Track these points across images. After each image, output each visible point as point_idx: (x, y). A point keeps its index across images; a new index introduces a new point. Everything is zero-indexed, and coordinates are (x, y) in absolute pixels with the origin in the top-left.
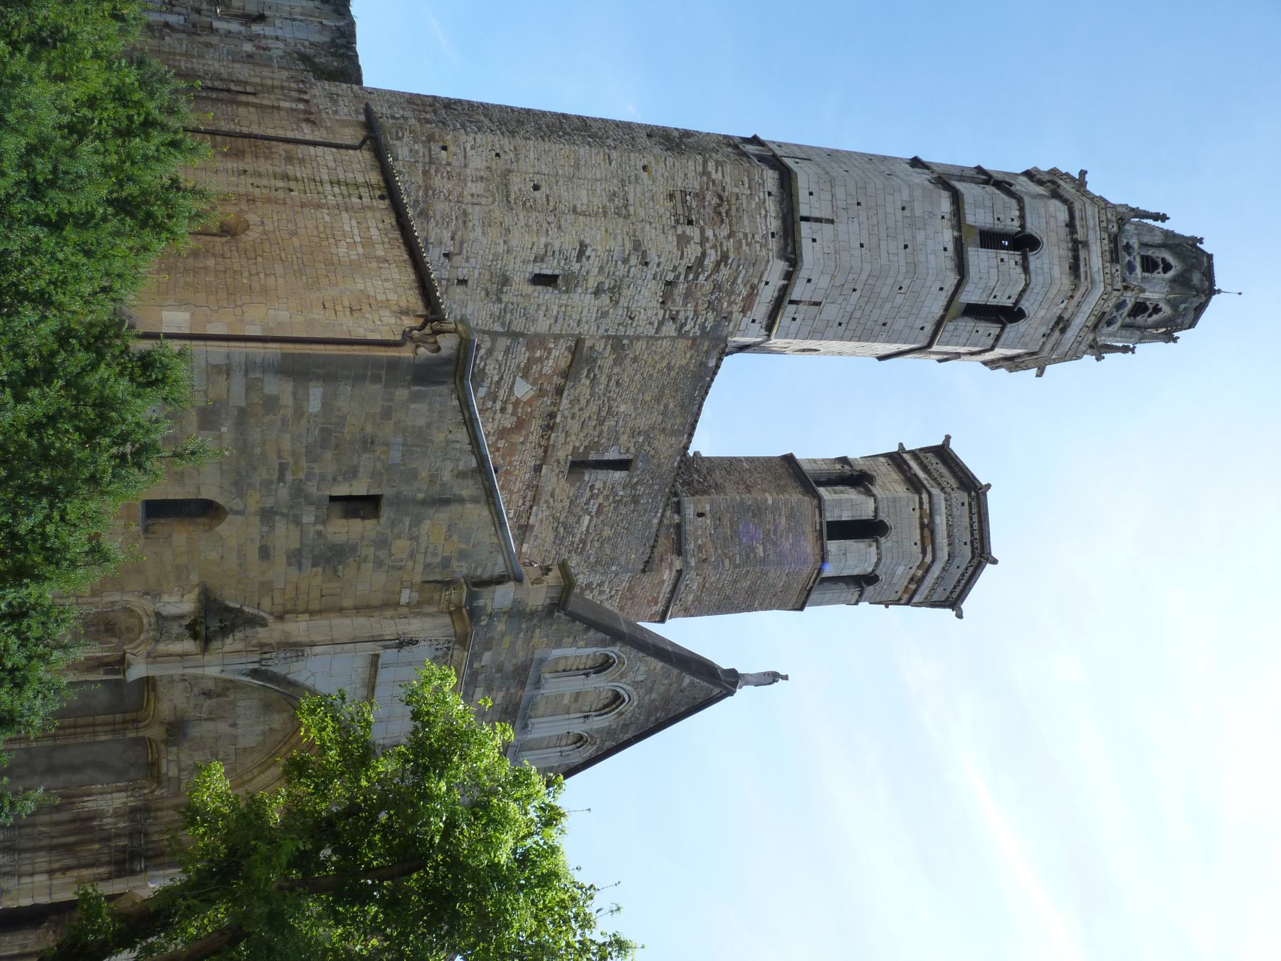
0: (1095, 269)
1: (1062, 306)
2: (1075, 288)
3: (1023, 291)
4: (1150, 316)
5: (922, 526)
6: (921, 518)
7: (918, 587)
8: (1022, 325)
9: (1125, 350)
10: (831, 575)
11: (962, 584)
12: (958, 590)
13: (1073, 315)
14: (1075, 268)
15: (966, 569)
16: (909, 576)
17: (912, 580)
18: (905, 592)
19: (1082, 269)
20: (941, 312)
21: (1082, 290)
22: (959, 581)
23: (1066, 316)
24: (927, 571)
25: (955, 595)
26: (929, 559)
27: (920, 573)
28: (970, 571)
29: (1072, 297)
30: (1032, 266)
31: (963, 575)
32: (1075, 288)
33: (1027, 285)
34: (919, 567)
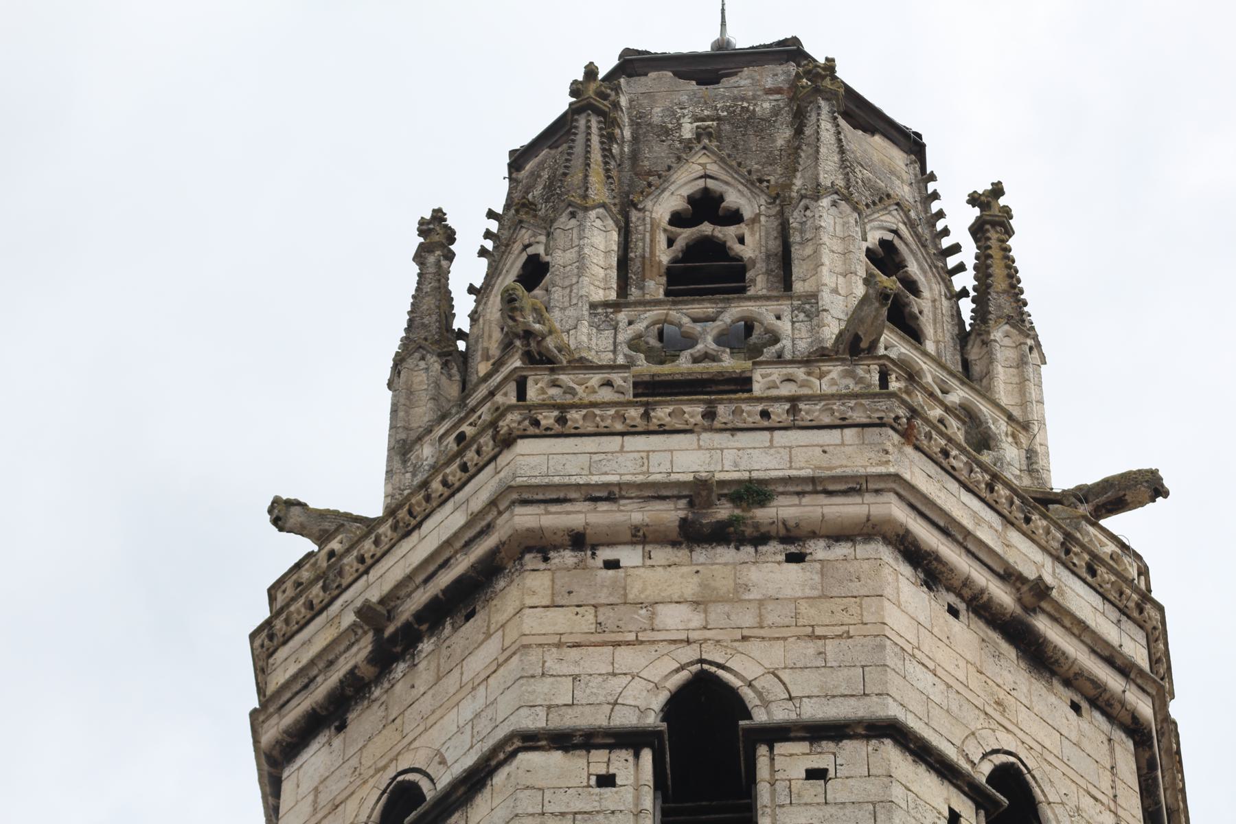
0: (459, 519)
1: (629, 556)
2: (539, 546)
3: (563, 741)
4: (735, 217)
8: (745, 669)
9: (992, 219)
13: (655, 492)
14: (463, 599)
19: (461, 566)
21: (526, 518)
23: (670, 514)
29: (578, 541)
30: (462, 761)
32: (539, 546)
33: (530, 741)
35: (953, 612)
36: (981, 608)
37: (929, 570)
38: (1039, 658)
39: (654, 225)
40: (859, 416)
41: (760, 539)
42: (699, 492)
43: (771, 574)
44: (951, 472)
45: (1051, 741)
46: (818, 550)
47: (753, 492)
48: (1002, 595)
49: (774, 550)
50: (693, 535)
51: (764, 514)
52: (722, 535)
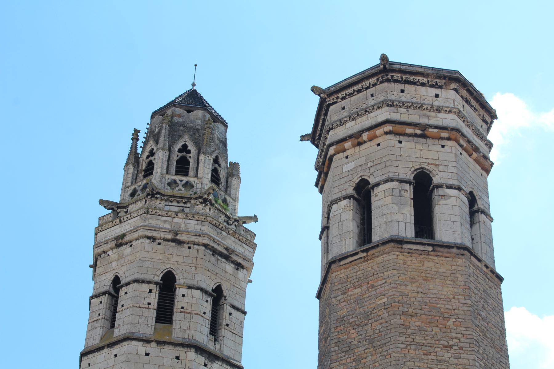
5: (326, 174)
6: (325, 180)
7: (362, 131)
10: (409, 211)
11: (356, 88)
12: (366, 83)
15: (343, 98)
16: (357, 149)
17: (359, 144)
18: (376, 137)
20: (106, 350)
22: (359, 91)
24: (344, 140)
25: (373, 80)
26: (332, 151)
27: (347, 145)
28: (343, 94)
31: (351, 95)
34: (344, 150)
35: (159, 244)
36: (166, 240)
37: (153, 239)
38: (180, 243)
39: (143, 160)
40: (139, 214)
41: (127, 243)
42: (117, 238)
43: (126, 250)
44: (159, 215)
45: (180, 259)
46: (134, 243)
47: (124, 235)
48: (170, 236)
49: (129, 244)
50: (118, 246)
51: (126, 239)
52: (121, 245)
